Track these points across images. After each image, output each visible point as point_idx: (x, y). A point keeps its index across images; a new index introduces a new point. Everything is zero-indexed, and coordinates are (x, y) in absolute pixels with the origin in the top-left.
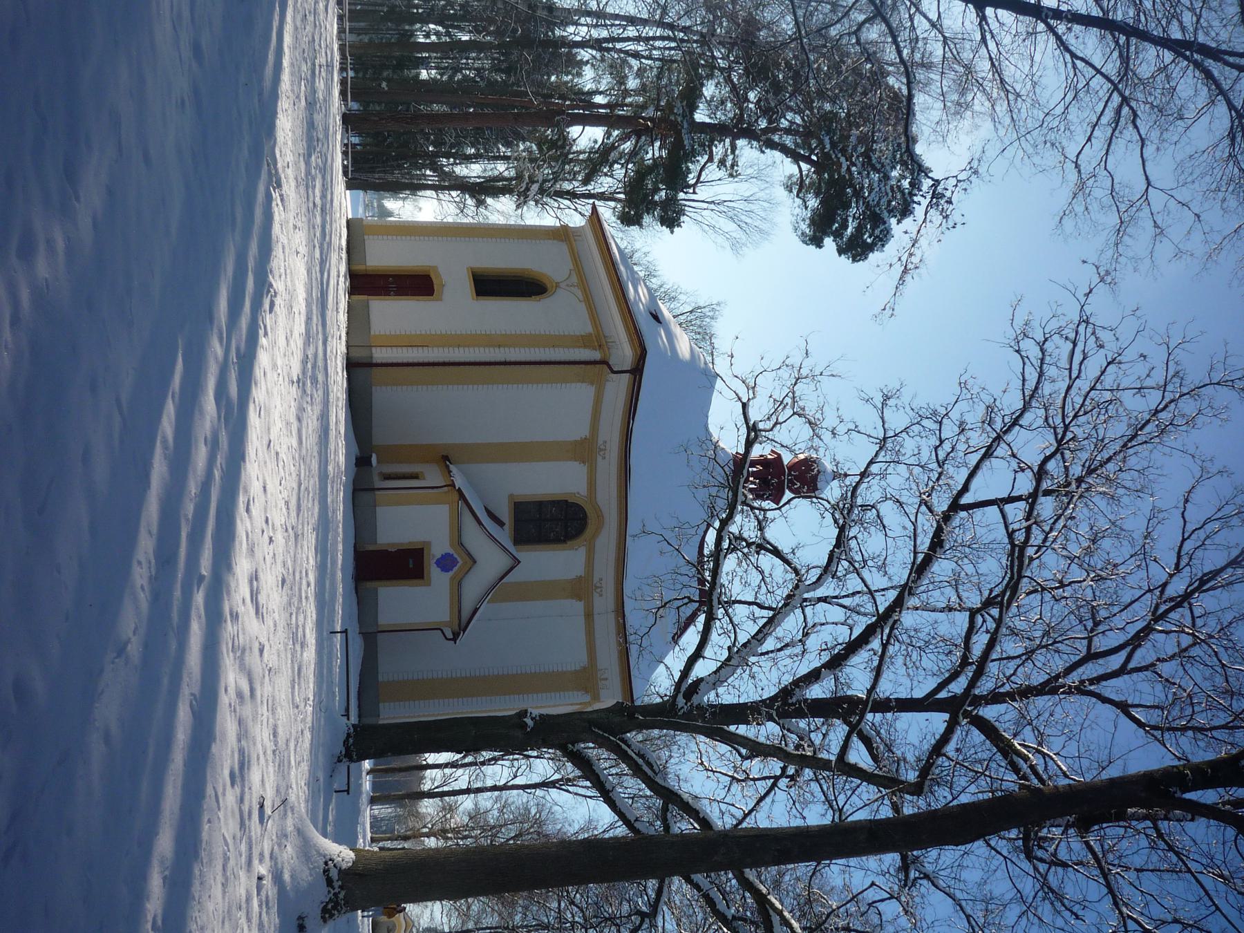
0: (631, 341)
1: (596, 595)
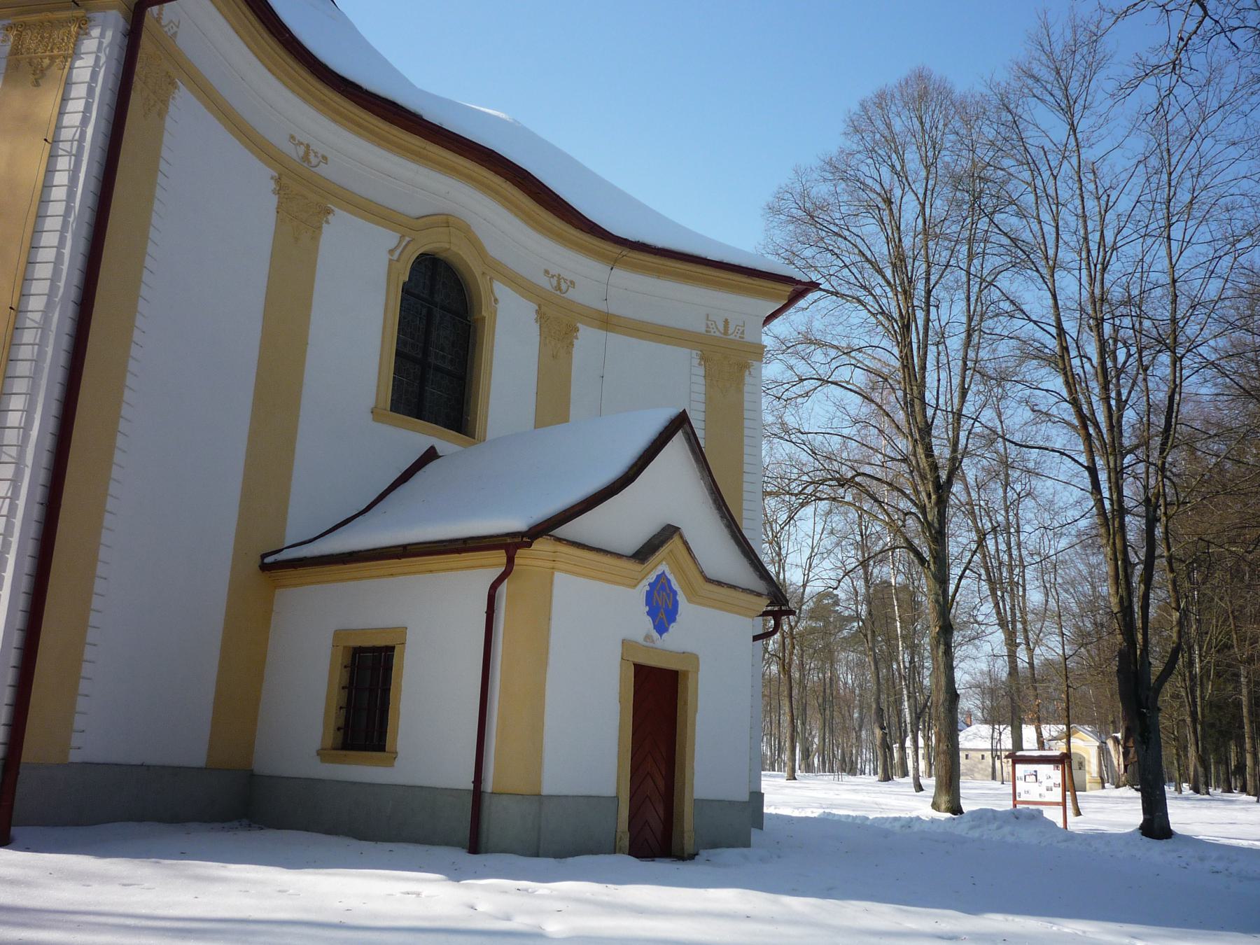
1: (572, 294)
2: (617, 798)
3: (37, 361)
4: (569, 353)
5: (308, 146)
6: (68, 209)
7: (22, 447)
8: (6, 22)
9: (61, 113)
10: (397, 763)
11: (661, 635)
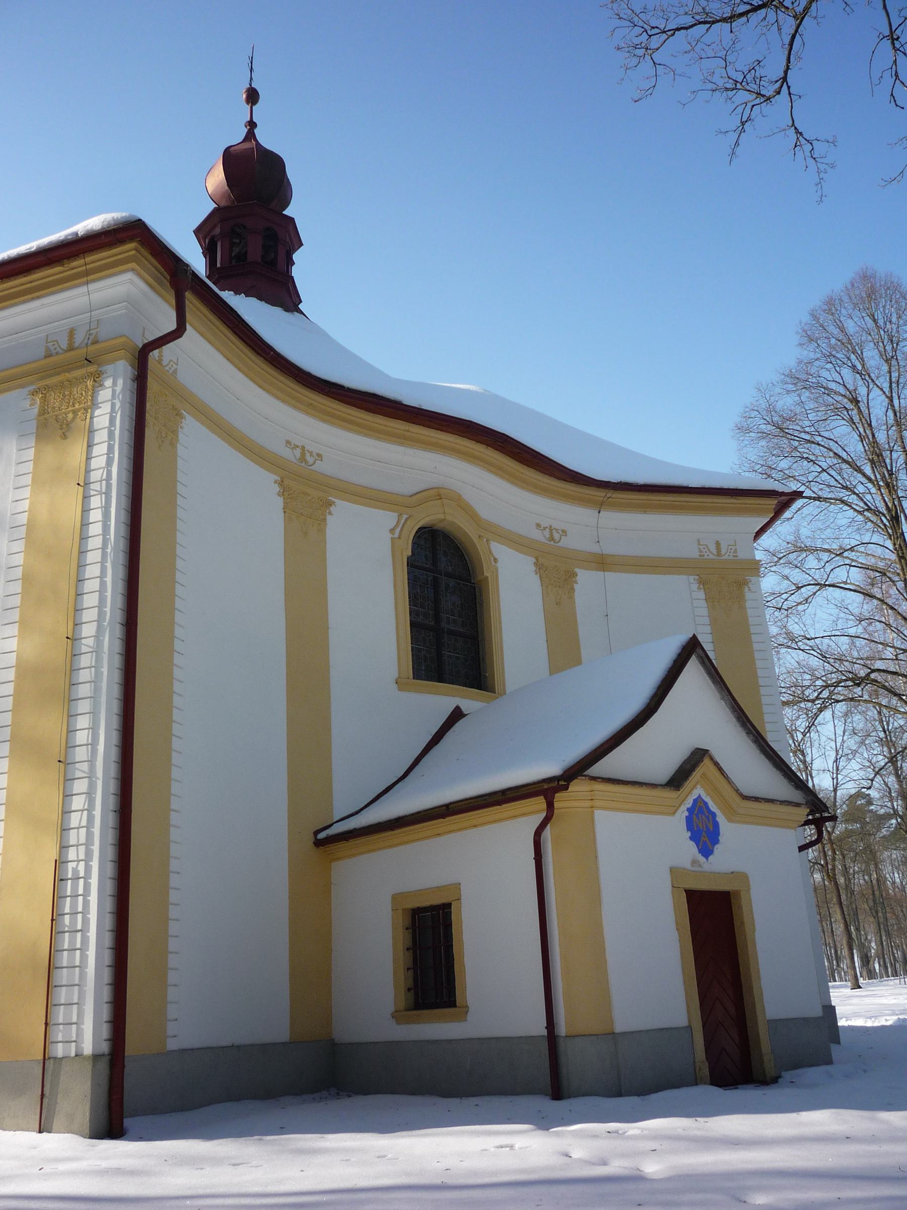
0: (87, 276)
1: (565, 542)
2: (690, 1027)
3: (96, 682)
4: (571, 597)
5: (303, 448)
6: (105, 542)
7: (92, 762)
8: (32, 388)
9: (89, 458)
10: (469, 1017)
11: (707, 860)
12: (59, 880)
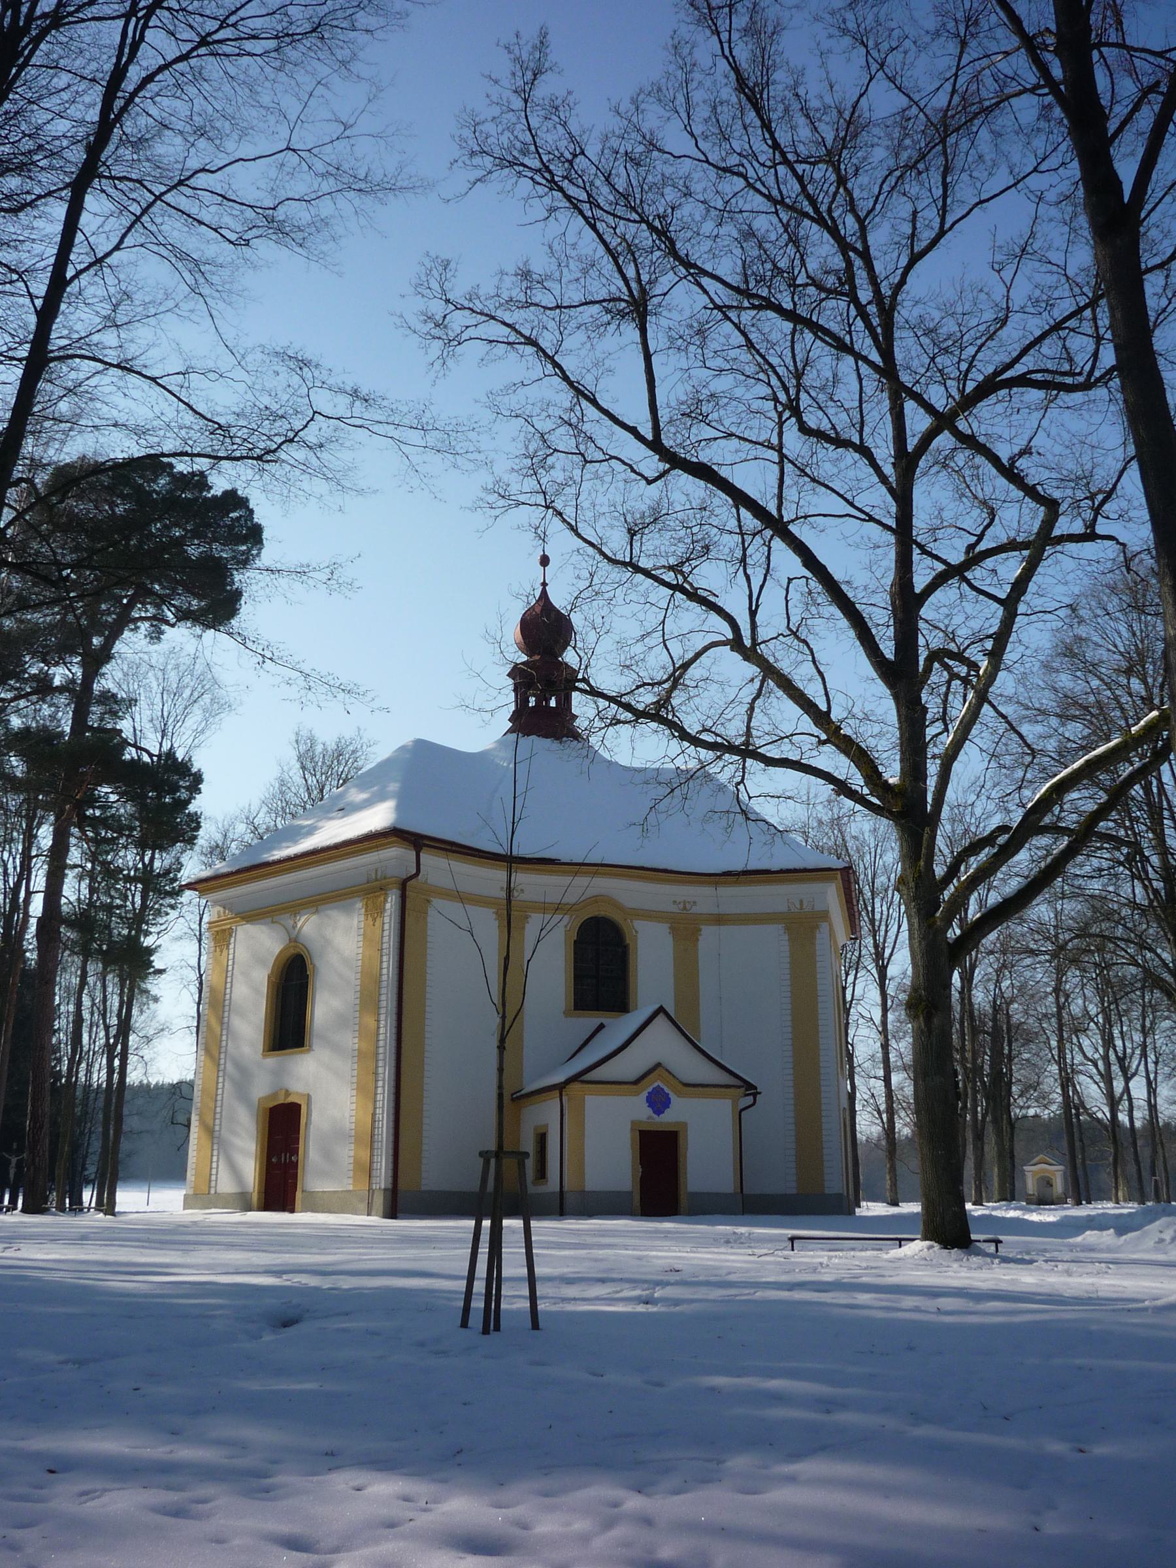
0: (377, 848)
1: (694, 910)
12: (374, 1121)
